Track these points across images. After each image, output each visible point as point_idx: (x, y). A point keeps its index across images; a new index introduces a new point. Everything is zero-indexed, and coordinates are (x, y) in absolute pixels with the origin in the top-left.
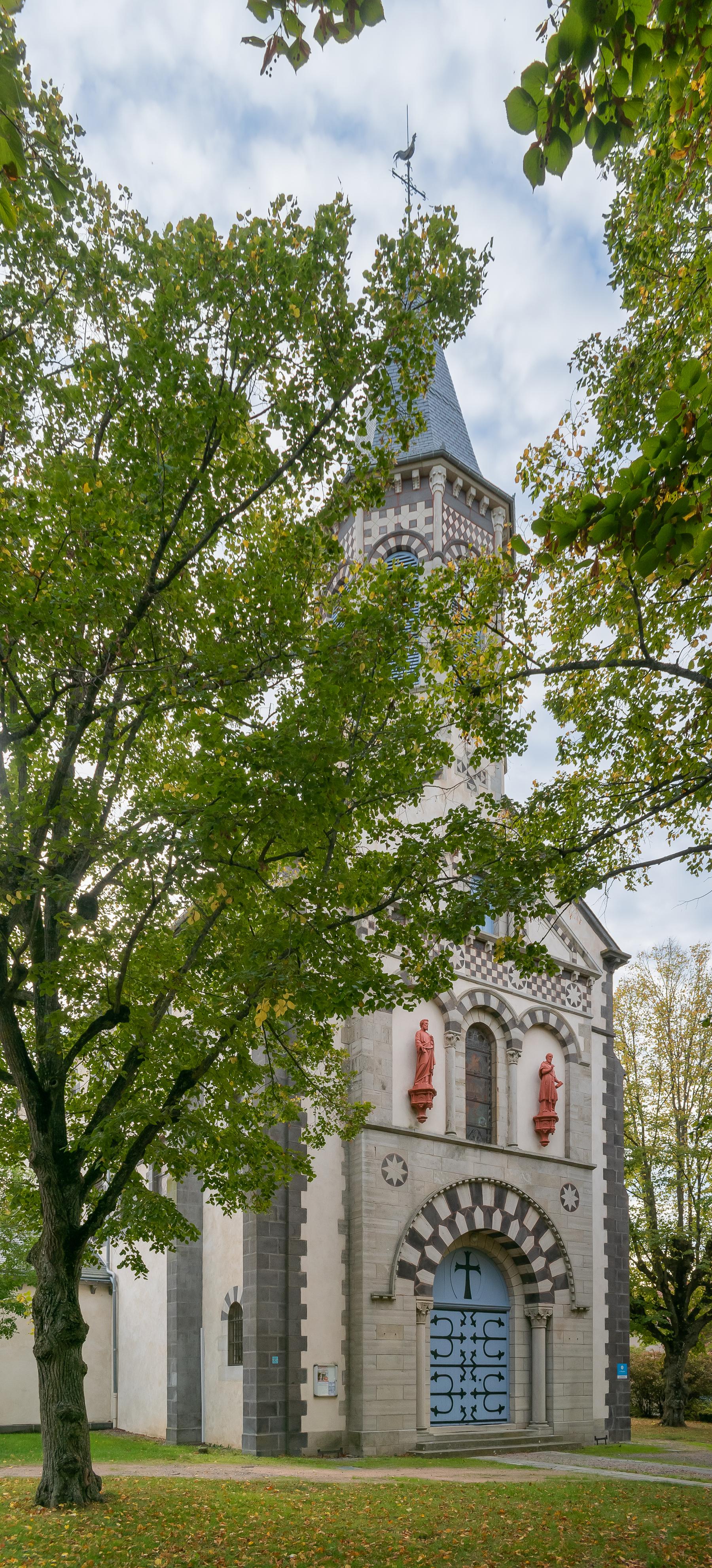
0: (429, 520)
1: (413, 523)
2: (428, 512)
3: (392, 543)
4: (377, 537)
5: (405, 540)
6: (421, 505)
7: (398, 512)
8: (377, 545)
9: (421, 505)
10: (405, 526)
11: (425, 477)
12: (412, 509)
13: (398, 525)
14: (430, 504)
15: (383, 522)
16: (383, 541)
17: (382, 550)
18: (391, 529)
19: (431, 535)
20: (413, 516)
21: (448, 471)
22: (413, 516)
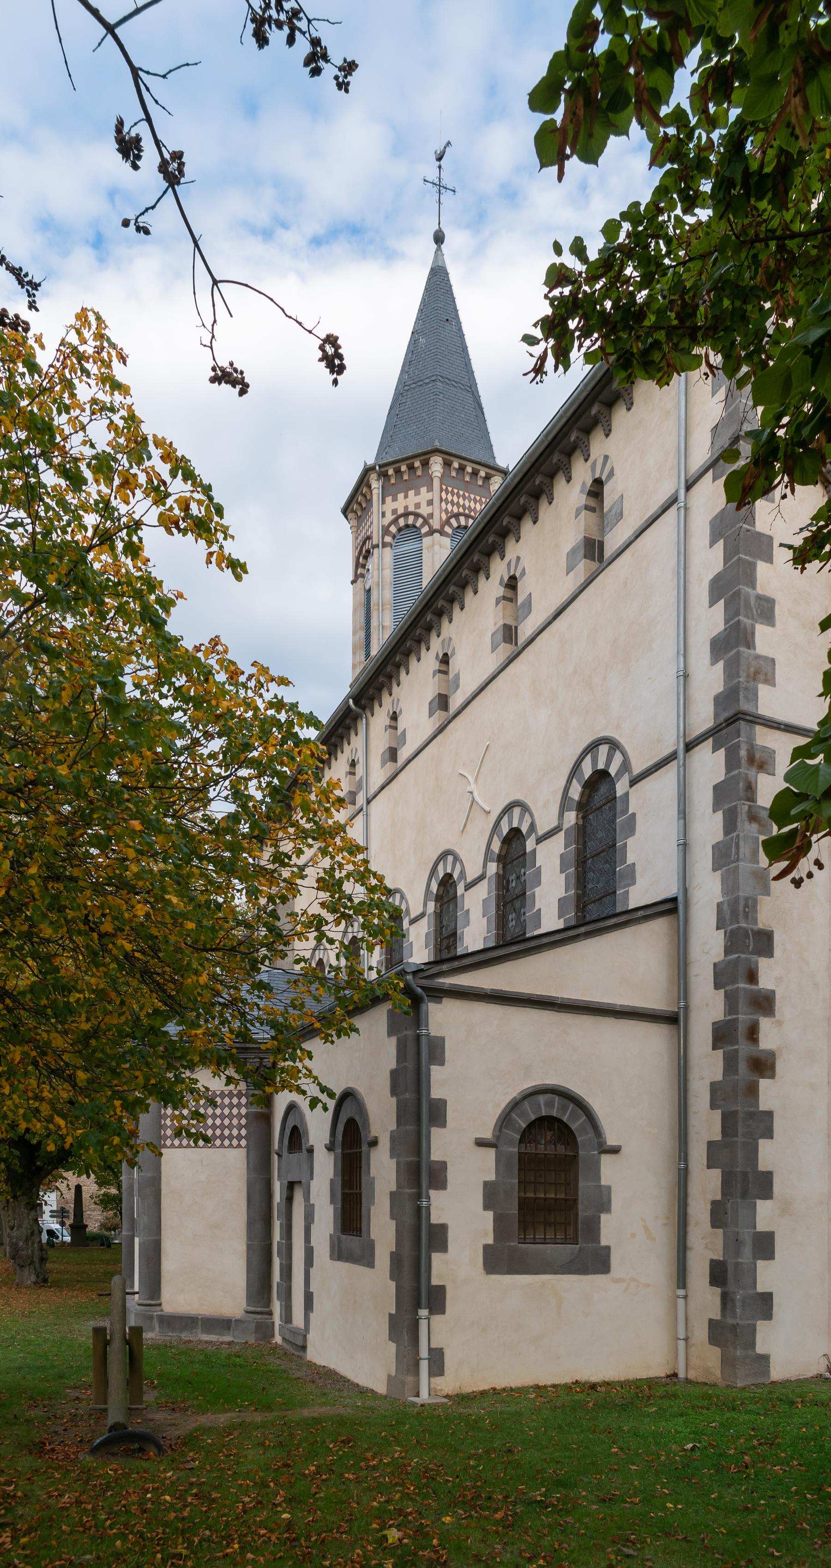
0: (430, 503)
1: (418, 505)
2: (429, 496)
3: (402, 522)
4: (390, 517)
5: (411, 520)
6: (424, 490)
7: (406, 497)
8: (390, 525)
9: (424, 490)
10: (411, 509)
11: (426, 464)
12: (417, 493)
13: (406, 507)
14: (430, 489)
15: (394, 505)
16: (395, 521)
17: (393, 529)
18: (401, 511)
19: (431, 515)
20: (417, 499)
21: (443, 459)
22: (417, 499)
